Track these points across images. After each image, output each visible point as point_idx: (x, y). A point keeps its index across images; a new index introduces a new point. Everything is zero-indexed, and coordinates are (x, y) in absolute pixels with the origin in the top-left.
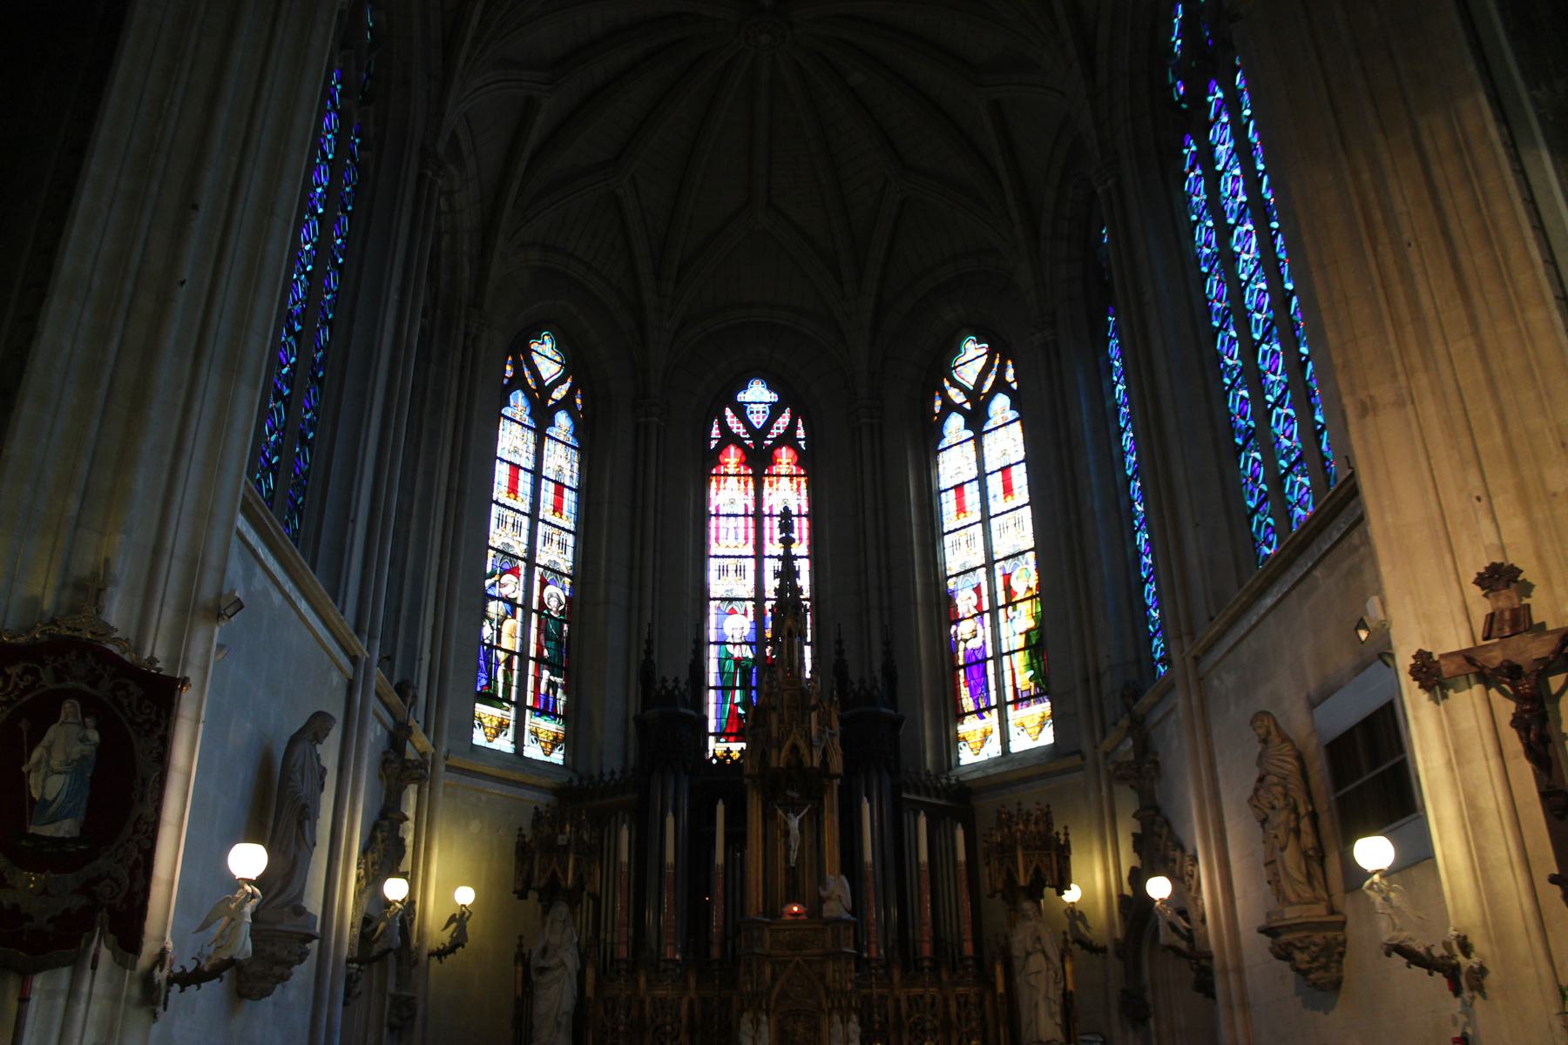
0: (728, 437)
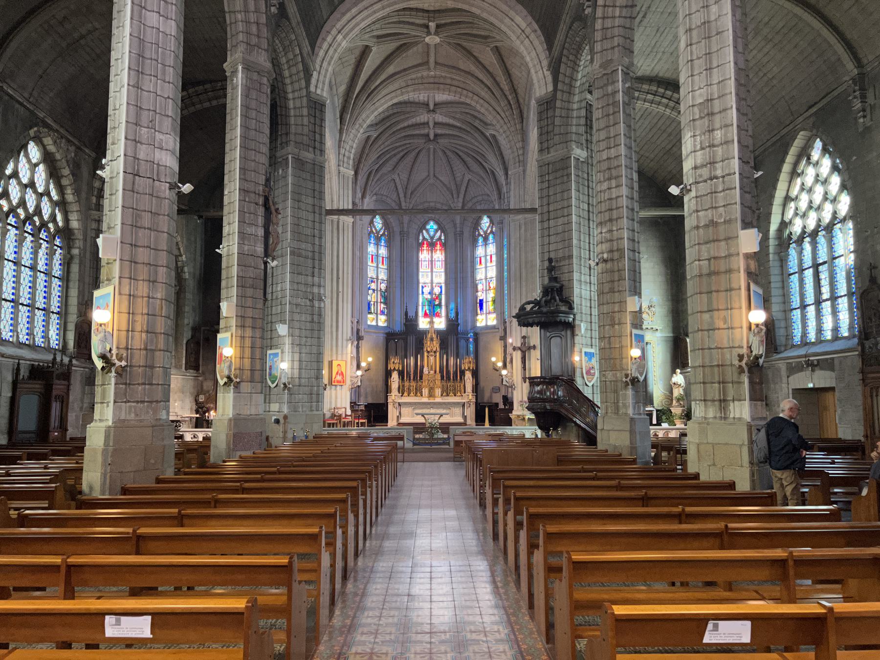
0: (424, 238)
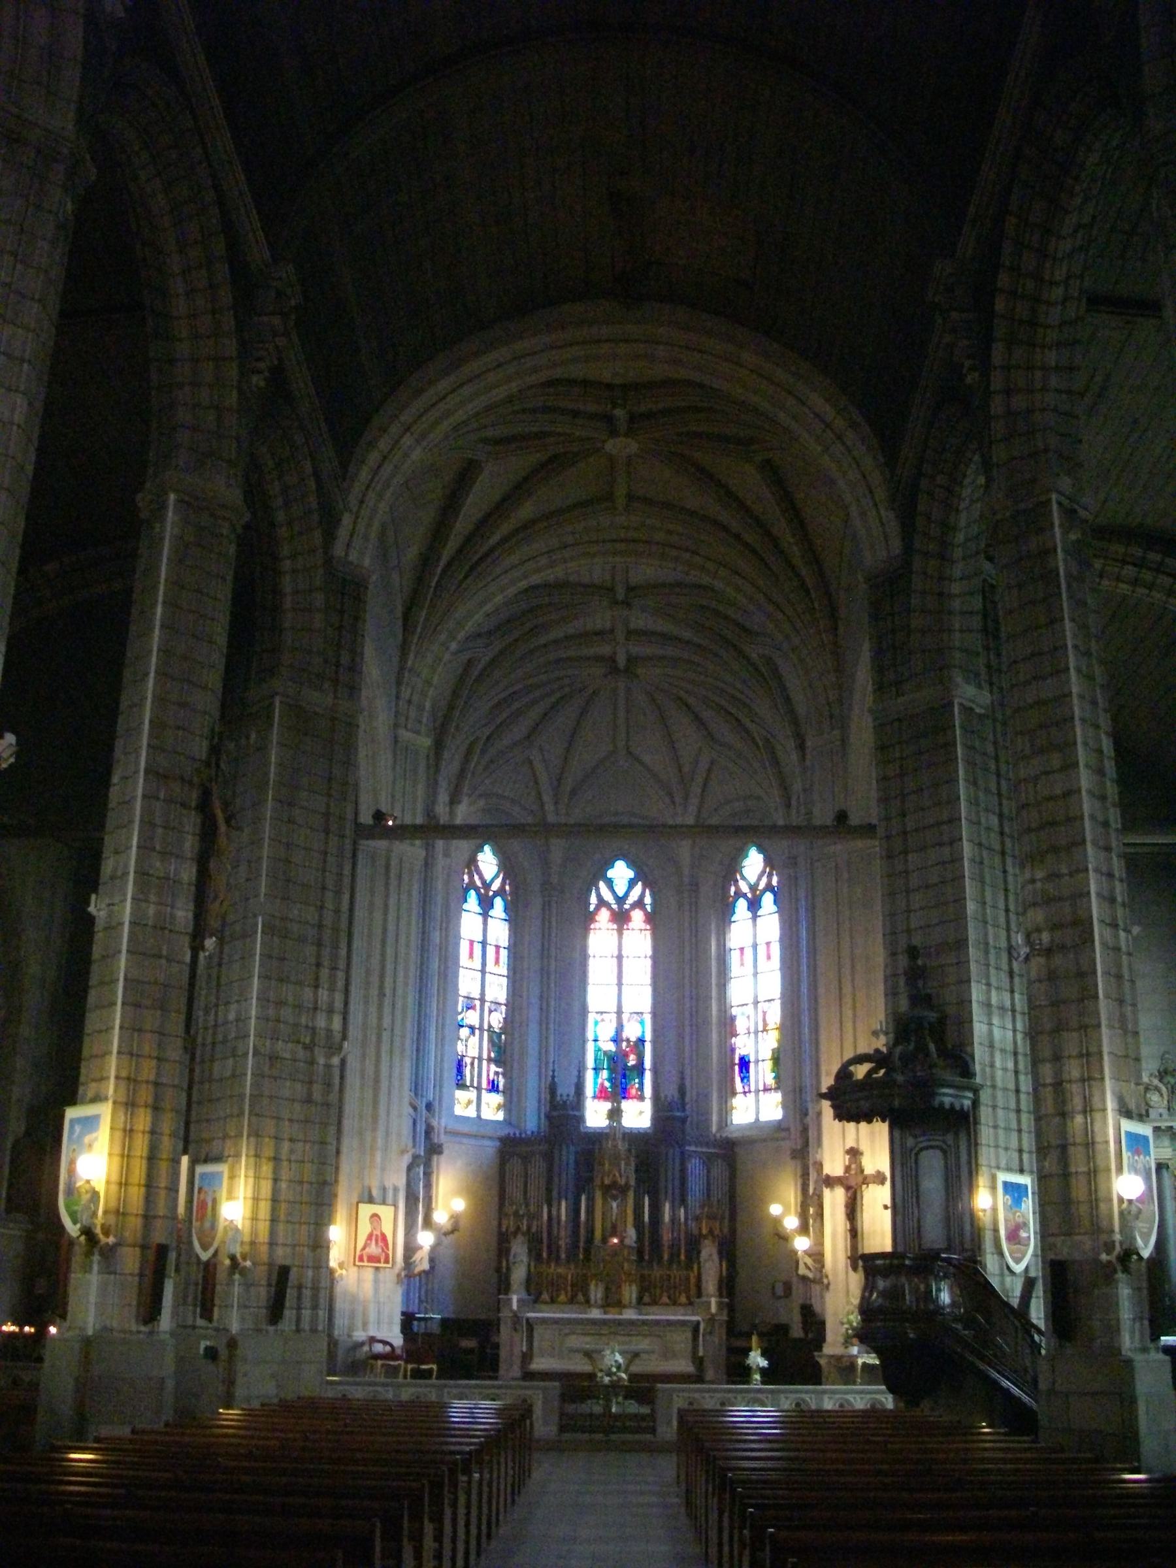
0: (602, 903)
